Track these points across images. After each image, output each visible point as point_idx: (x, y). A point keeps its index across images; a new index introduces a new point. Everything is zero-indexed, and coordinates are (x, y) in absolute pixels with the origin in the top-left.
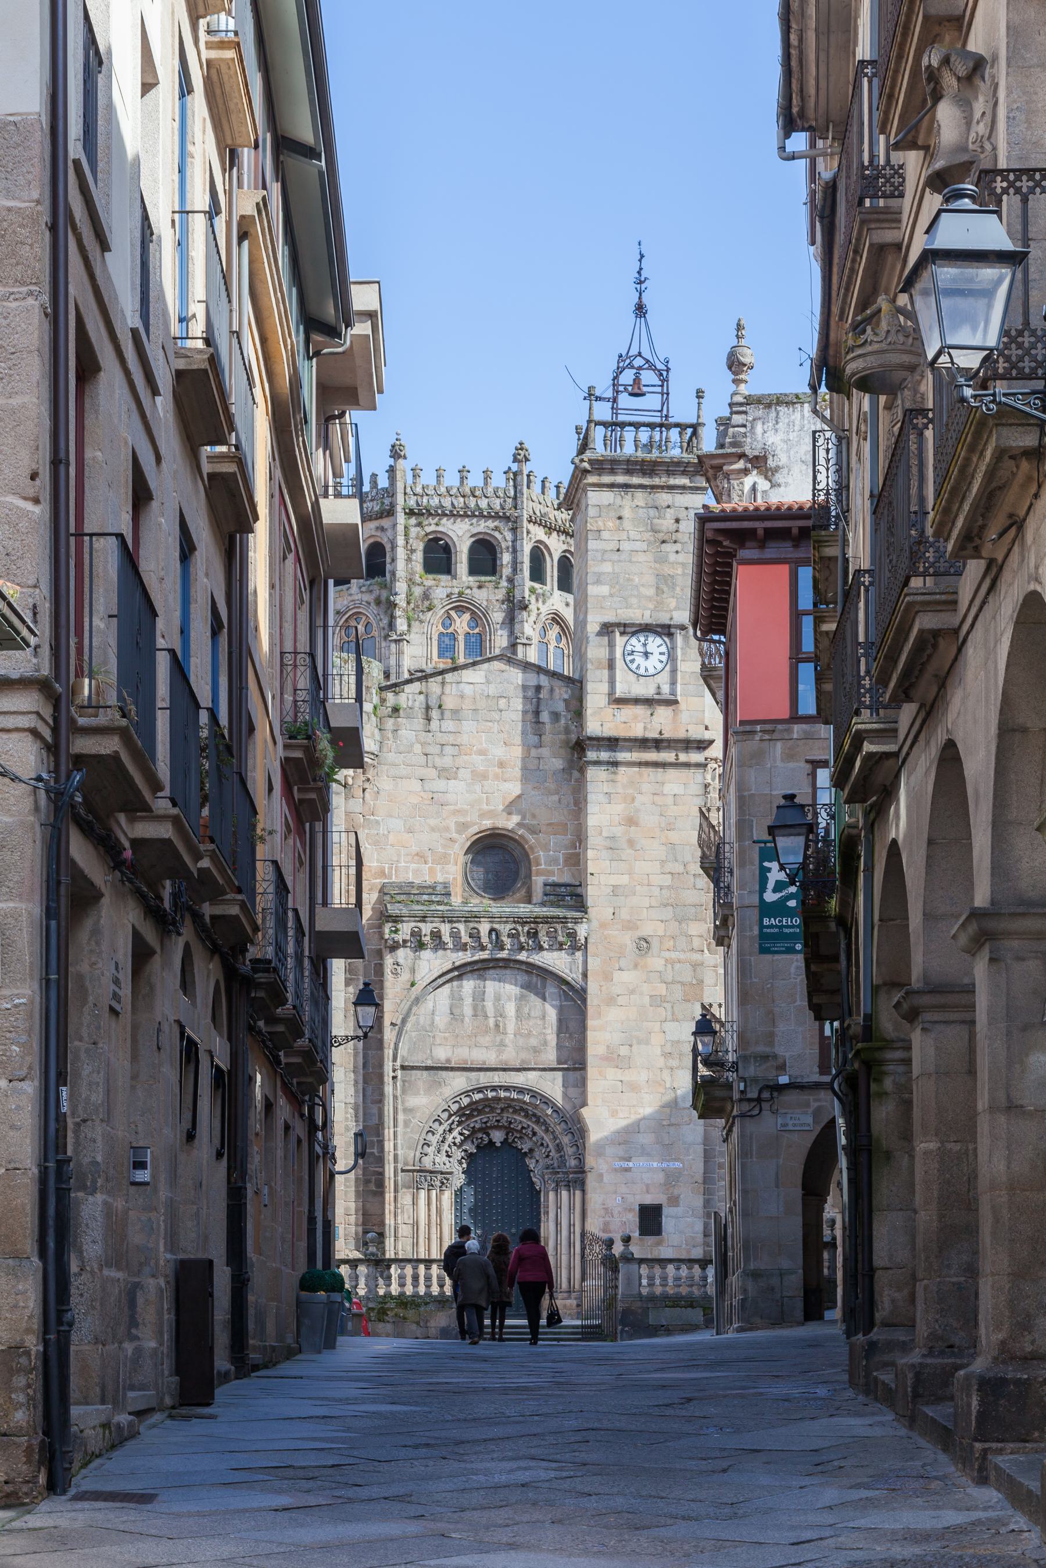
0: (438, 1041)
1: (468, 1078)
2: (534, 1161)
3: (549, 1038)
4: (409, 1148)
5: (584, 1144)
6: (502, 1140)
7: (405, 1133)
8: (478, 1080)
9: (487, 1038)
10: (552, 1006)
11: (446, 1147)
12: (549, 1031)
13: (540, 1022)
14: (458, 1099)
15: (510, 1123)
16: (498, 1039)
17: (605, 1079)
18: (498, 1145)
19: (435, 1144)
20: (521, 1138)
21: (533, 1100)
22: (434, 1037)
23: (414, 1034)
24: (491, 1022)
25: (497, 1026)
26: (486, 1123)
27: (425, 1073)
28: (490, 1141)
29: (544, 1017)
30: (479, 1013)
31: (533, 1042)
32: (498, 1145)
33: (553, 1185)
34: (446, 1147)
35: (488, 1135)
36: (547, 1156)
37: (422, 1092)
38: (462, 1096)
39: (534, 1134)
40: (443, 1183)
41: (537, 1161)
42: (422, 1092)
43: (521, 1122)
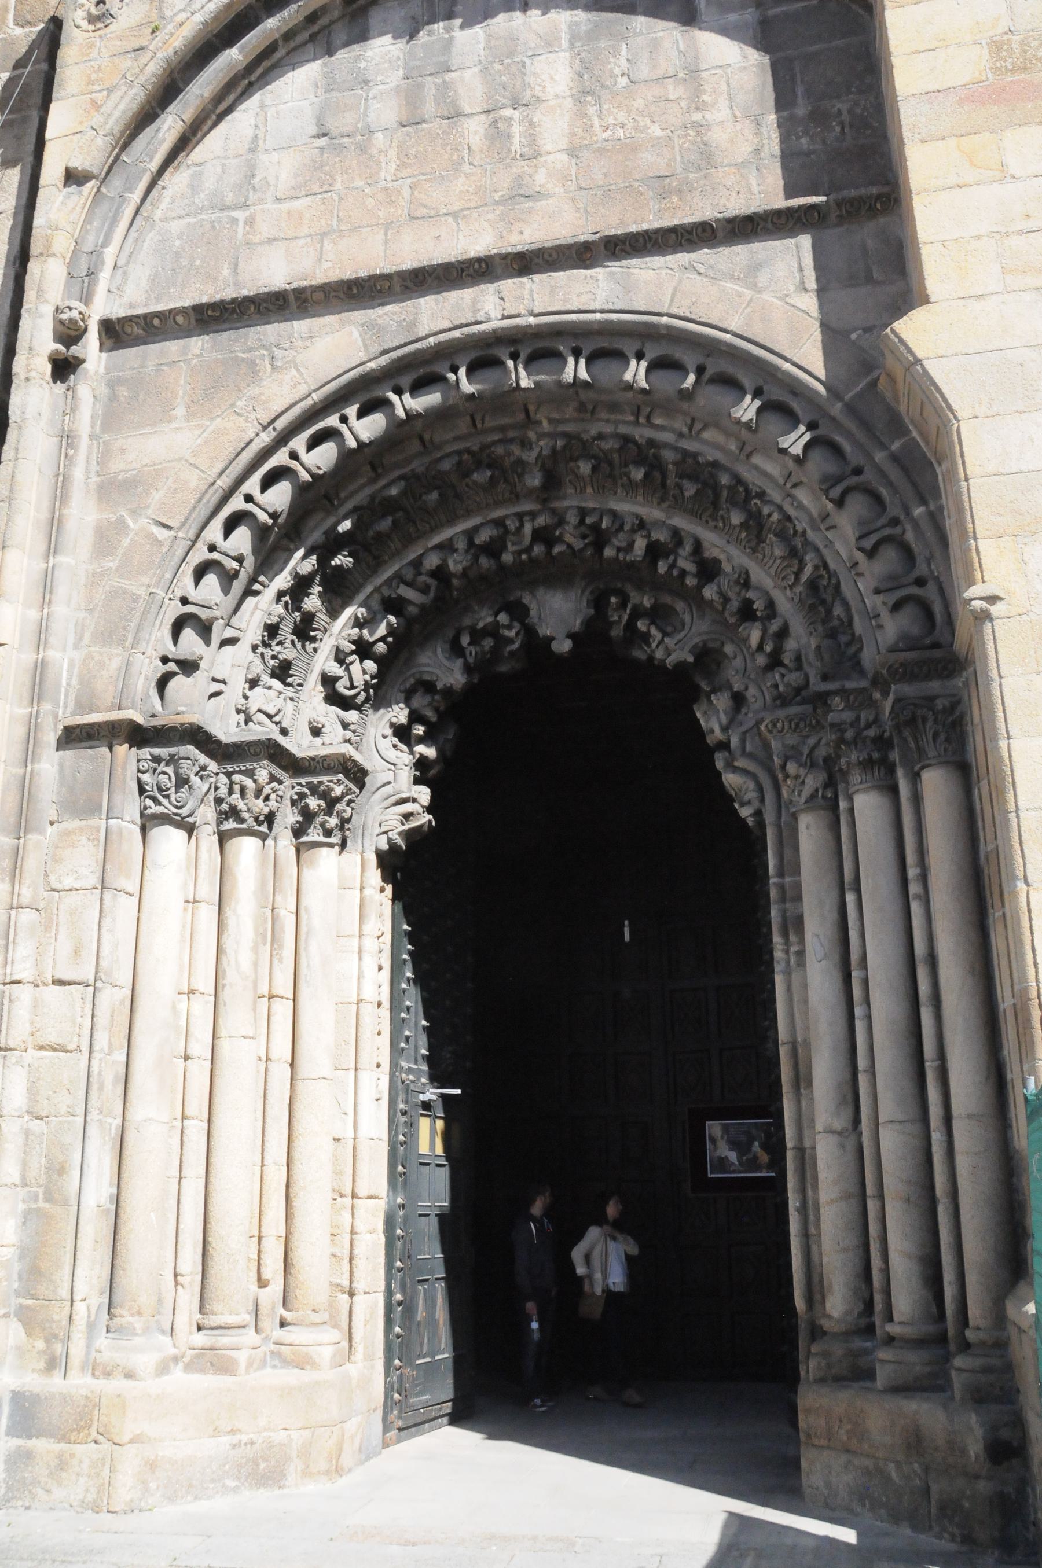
0: (264, 229)
1: (368, 326)
2: (722, 701)
3: (718, 136)
4: (108, 636)
5: (936, 520)
6: (577, 625)
7: (95, 579)
8: (413, 324)
9: (460, 184)
10: (724, 31)
11: (323, 661)
12: (719, 113)
13: (674, 91)
14: (333, 421)
15: (599, 539)
16: (504, 182)
17: (1004, 175)
18: (563, 646)
19: (254, 633)
20: (659, 614)
21: (665, 381)
22: (250, 222)
23: (176, 227)
24: (475, 129)
25: (498, 133)
26: (493, 549)
27: (198, 344)
28: (530, 632)
29: (694, 72)
30: (429, 108)
31: (652, 161)
32: (563, 646)
33: (813, 781)
34: (323, 661)
35: (518, 612)
36: (775, 661)
37: (180, 411)
38: (352, 411)
39: (708, 570)
40: (308, 816)
41: (739, 700)
42: (180, 411)
43: (641, 525)
